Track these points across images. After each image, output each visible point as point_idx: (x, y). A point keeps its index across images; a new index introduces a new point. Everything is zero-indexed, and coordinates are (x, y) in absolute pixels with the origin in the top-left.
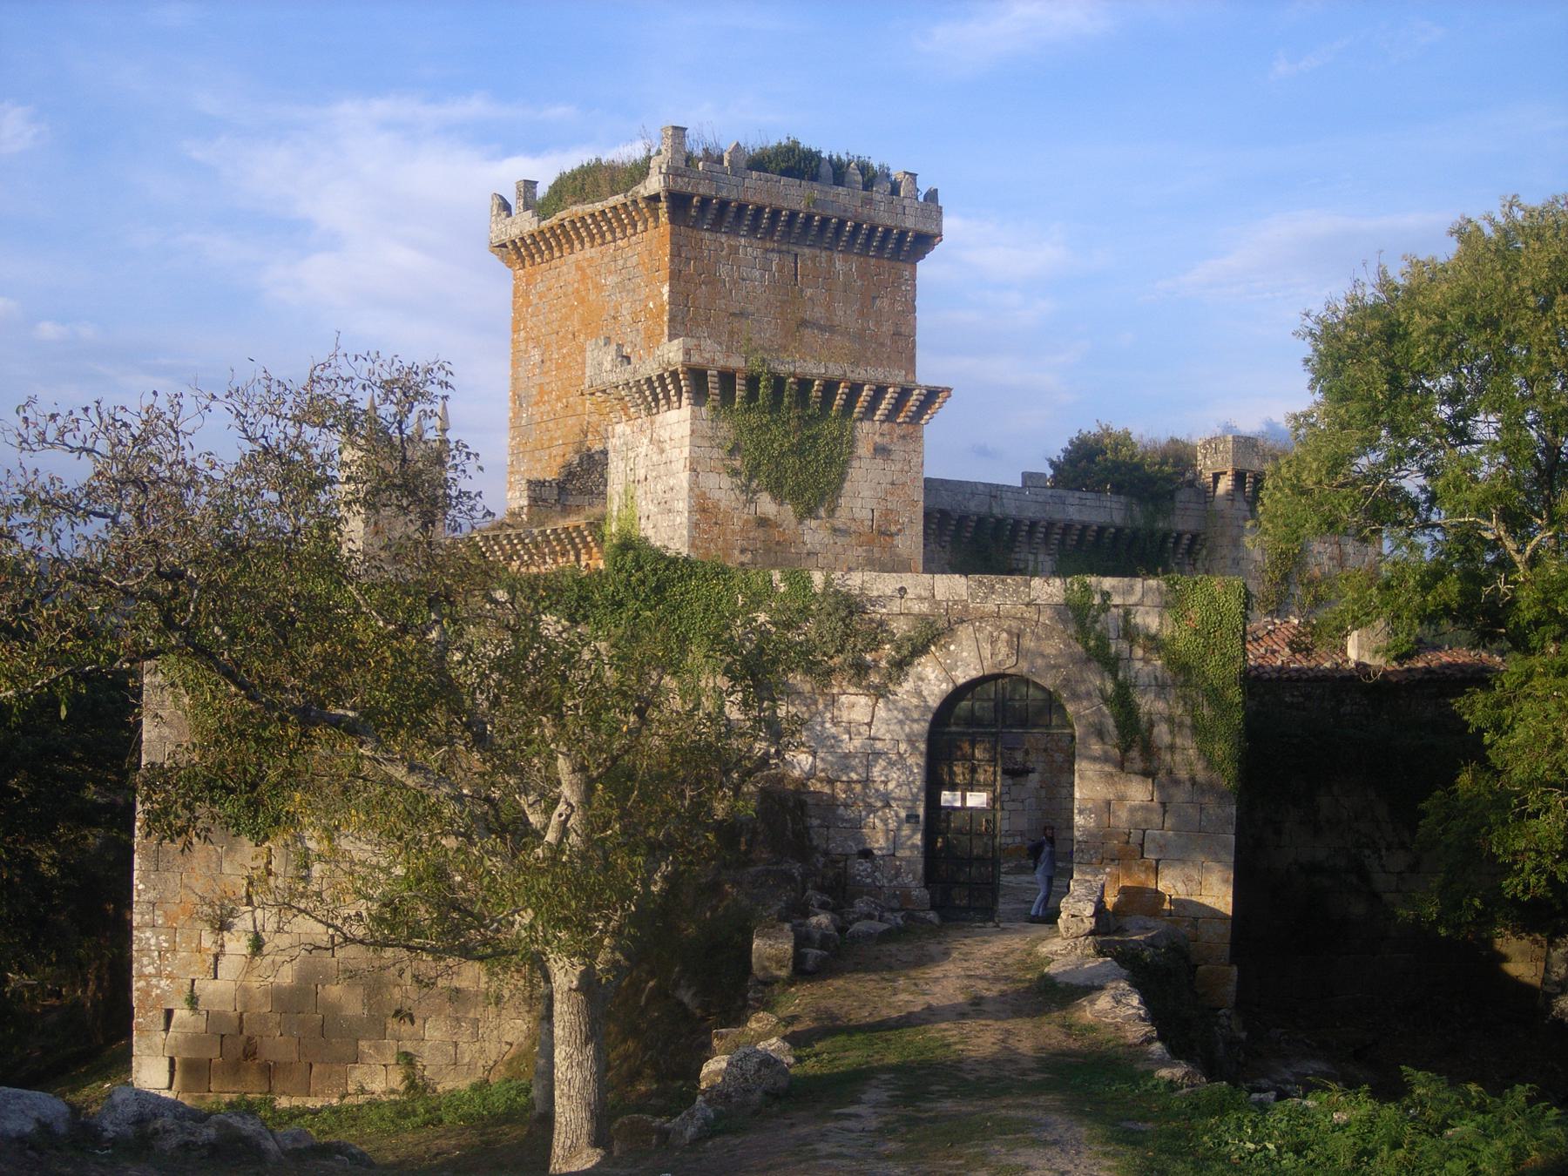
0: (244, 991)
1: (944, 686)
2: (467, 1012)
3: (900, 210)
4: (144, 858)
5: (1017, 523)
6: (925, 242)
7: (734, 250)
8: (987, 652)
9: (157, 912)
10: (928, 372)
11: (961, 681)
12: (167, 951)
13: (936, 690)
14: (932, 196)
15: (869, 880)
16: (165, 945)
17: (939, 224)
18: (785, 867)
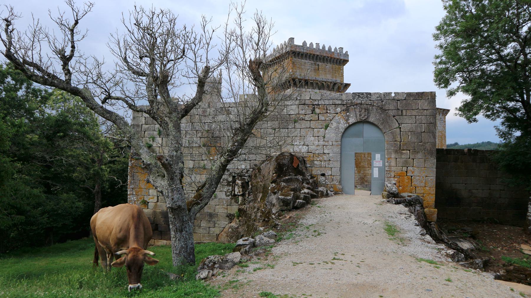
0: (155, 213)
1: (346, 125)
2: (212, 219)
4: (131, 176)
6: (345, 61)
7: (305, 63)
8: (358, 116)
9: (134, 191)
10: (346, 81)
11: (350, 124)
12: (136, 201)
13: (343, 127)
14: (347, 52)
15: (324, 183)
16: (135, 199)
17: (348, 58)
18: (297, 177)
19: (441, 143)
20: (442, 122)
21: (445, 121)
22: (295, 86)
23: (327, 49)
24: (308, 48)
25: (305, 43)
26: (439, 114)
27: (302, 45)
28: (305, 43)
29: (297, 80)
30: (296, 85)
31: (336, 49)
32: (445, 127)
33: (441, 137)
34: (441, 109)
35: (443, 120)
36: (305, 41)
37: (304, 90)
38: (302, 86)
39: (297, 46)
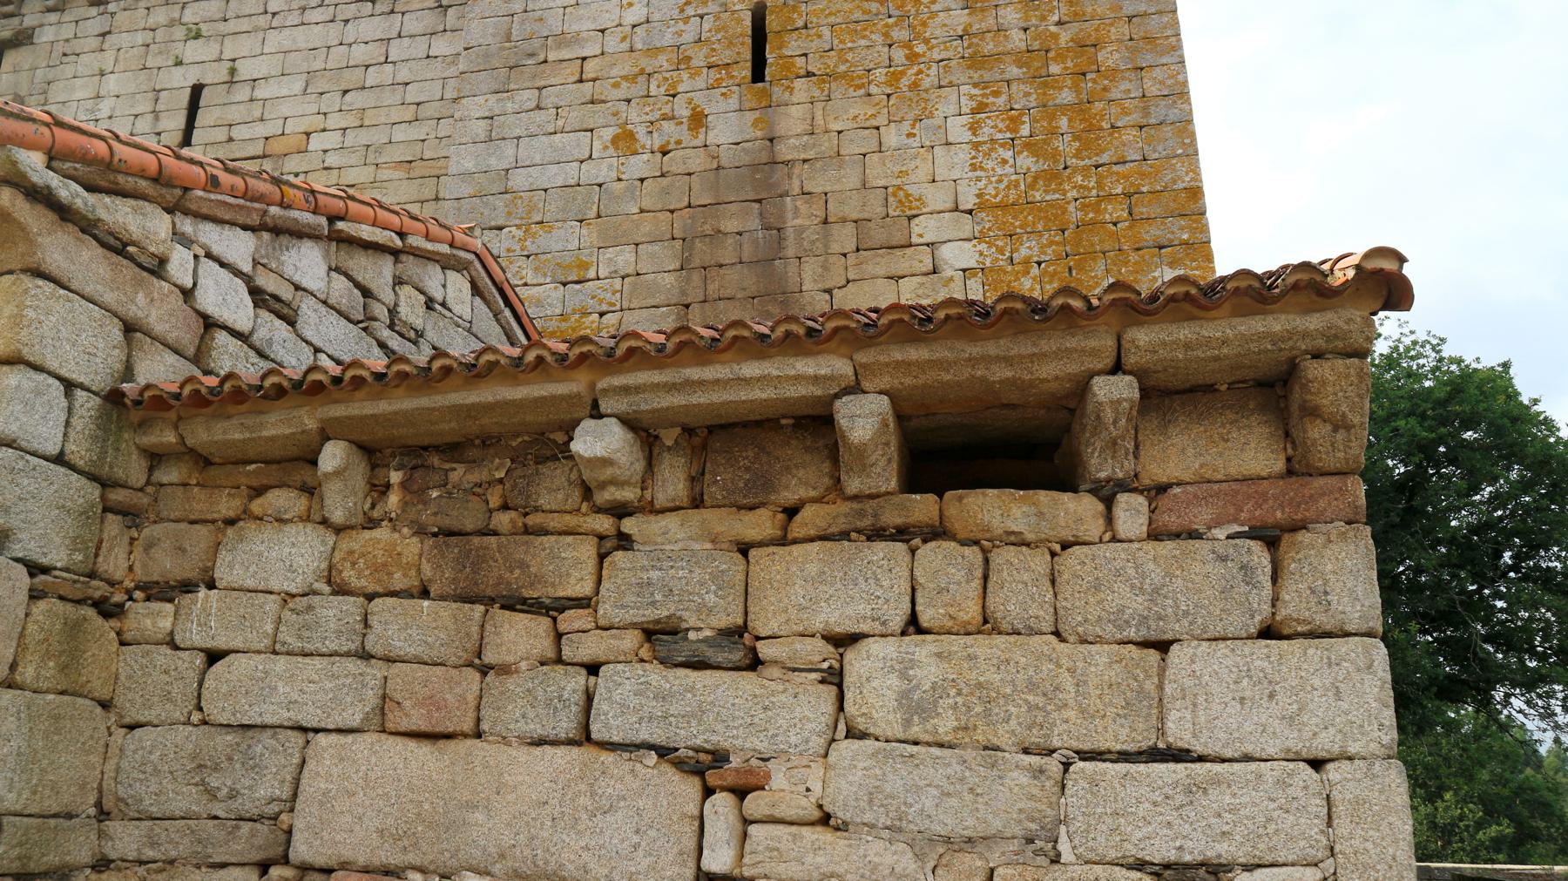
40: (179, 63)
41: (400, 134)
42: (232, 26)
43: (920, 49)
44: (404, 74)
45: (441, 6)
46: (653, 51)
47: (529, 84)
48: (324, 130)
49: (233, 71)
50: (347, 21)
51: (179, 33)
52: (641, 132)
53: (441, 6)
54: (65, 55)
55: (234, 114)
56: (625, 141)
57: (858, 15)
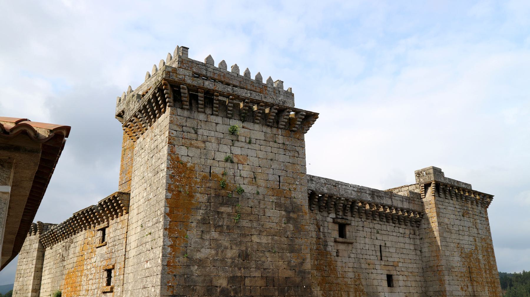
3: (277, 92)
5: (347, 200)
19: (489, 262)
20: (484, 219)
21: (487, 219)
22: (178, 104)
23: (253, 77)
24: (215, 69)
25: (209, 59)
26: (477, 203)
27: (203, 61)
28: (209, 59)
29: (183, 88)
30: (182, 101)
31: (270, 79)
32: (489, 229)
33: (487, 251)
34: (480, 194)
35: (484, 216)
36: (210, 56)
37: (202, 117)
38: (198, 108)
39: (192, 62)
40: (377, 239)
41: (410, 266)
42: (383, 232)
43: (483, 279)
44: (408, 253)
45: (410, 238)
46: (462, 272)
47: (451, 275)
48: (400, 262)
49: (385, 244)
50: (398, 237)
51: (375, 231)
52: (463, 287)
53: (410, 238)
54: (357, 230)
55: (387, 254)
56: (462, 288)
57: (477, 272)
